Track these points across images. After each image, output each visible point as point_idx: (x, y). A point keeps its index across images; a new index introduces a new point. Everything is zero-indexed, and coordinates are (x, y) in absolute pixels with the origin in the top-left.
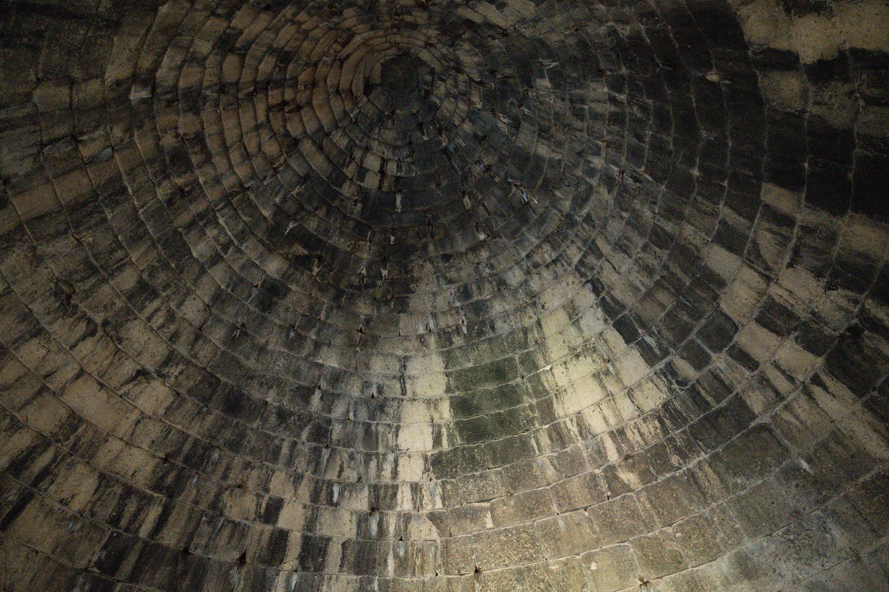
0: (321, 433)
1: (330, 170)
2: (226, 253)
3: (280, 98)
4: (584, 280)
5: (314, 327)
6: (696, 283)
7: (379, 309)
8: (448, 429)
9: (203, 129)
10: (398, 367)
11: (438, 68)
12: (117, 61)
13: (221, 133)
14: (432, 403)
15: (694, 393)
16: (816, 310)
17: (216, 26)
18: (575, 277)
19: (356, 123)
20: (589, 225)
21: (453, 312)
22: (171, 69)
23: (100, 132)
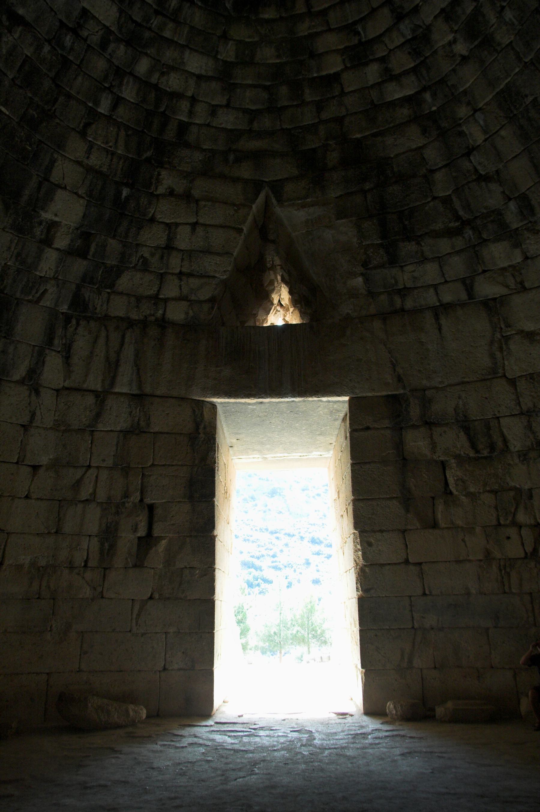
17: (351, 82)
23: (464, 128)
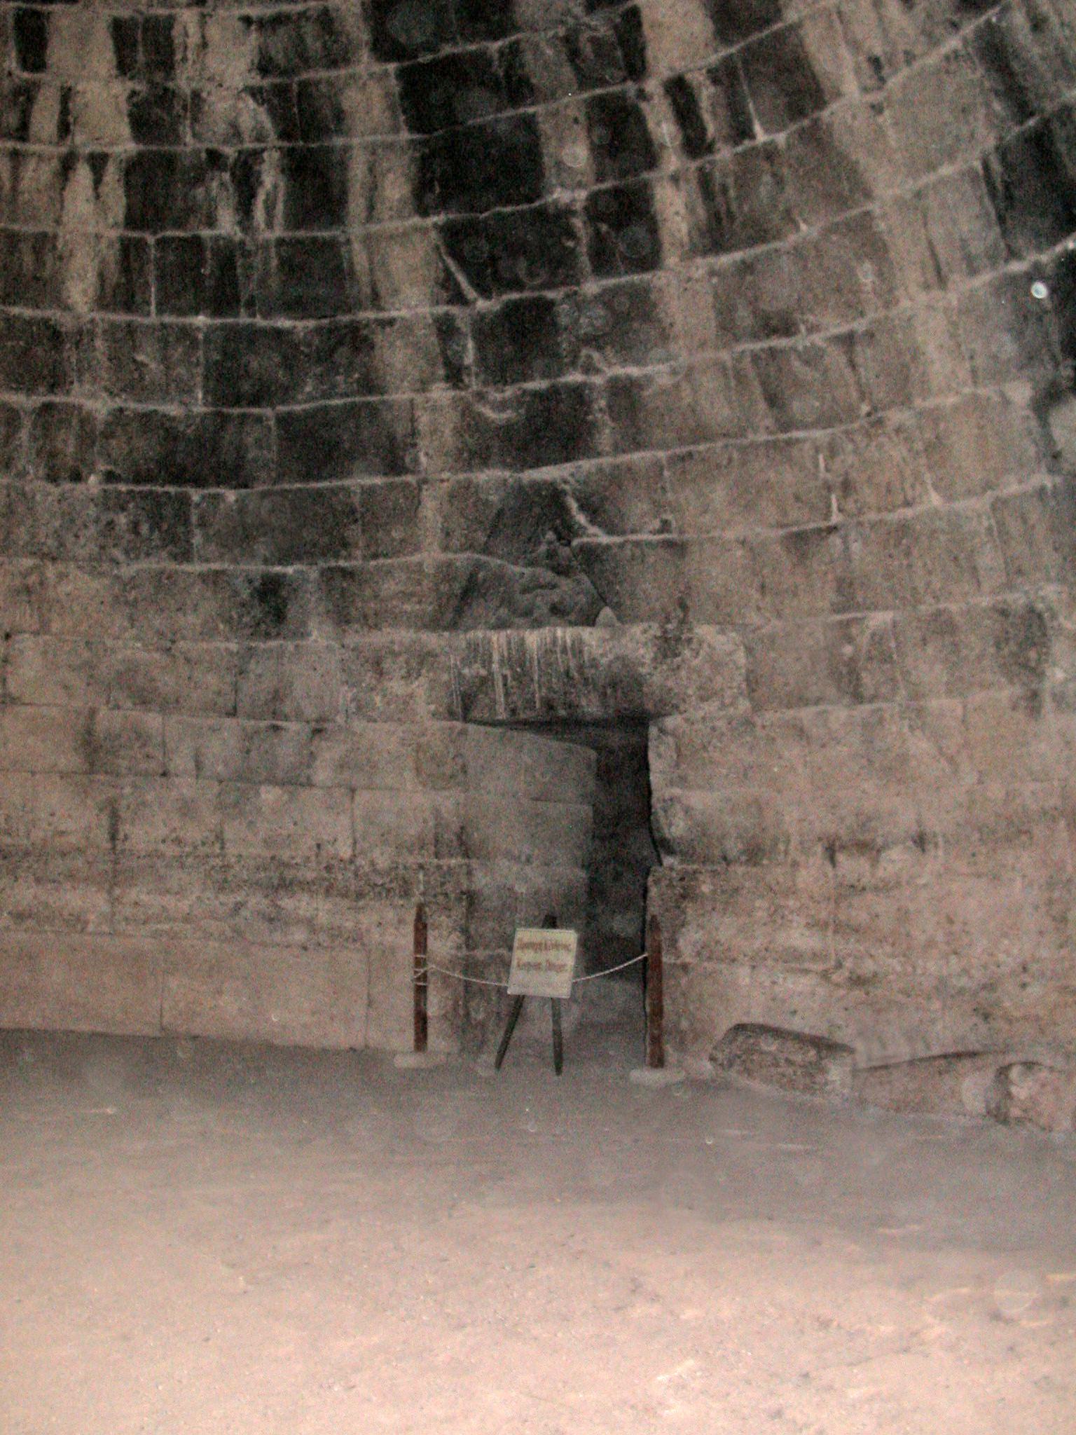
16: (204, 95)
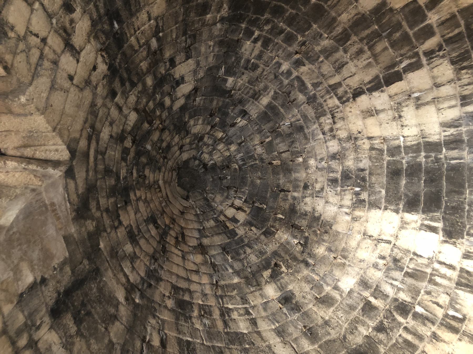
0: (403, 309)
1: (225, 236)
2: (252, 314)
3: (173, 238)
4: (351, 100)
5: (322, 285)
6: (378, 21)
7: (324, 241)
8: (426, 219)
9: (172, 283)
10: (369, 241)
11: (193, 153)
12: (116, 290)
13: (178, 276)
14: (404, 225)
15: (449, 41)
18: (347, 106)
19: (204, 212)
20: (319, 86)
21: (343, 193)
22: (132, 272)
23: (149, 329)
